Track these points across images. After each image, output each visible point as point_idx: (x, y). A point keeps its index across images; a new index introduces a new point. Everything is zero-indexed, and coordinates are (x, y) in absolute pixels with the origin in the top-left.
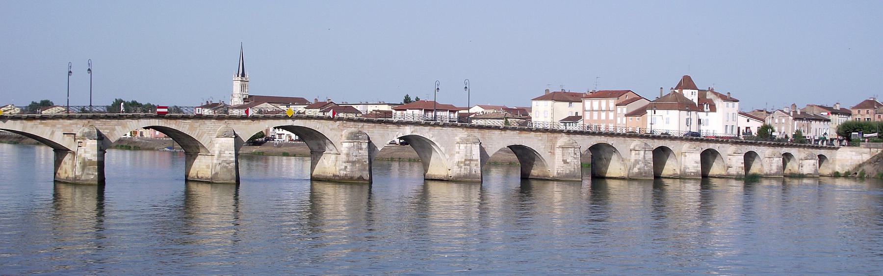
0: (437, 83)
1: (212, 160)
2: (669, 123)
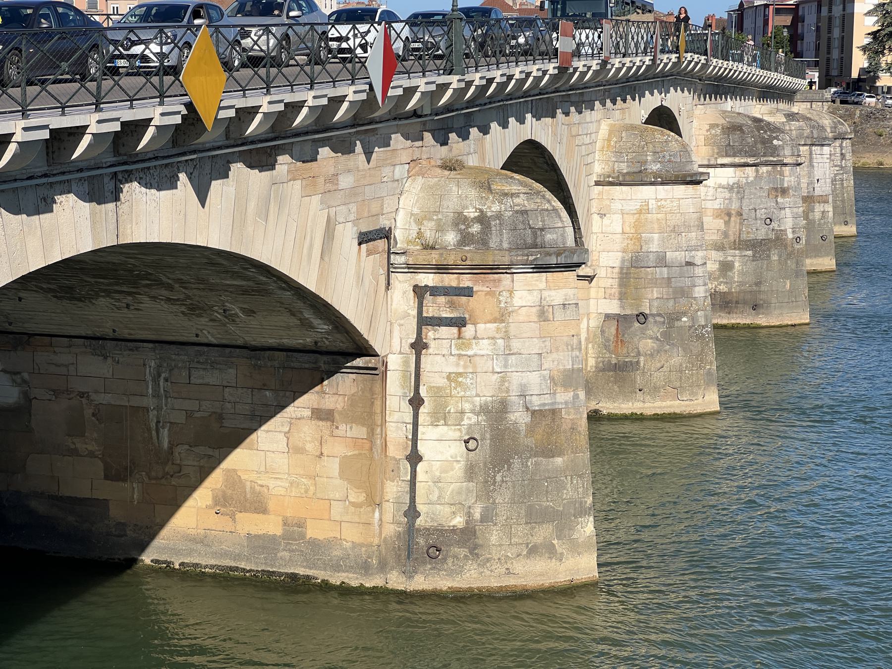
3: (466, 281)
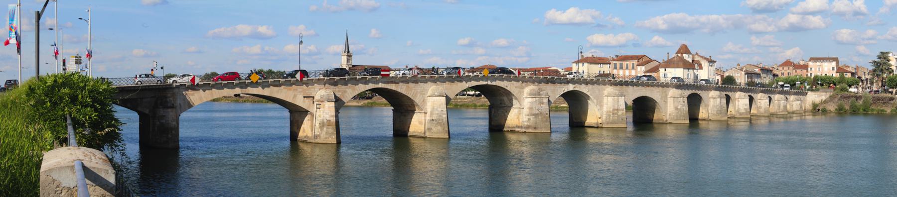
0: (581, 47)
1: (425, 117)
3: (321, 103)
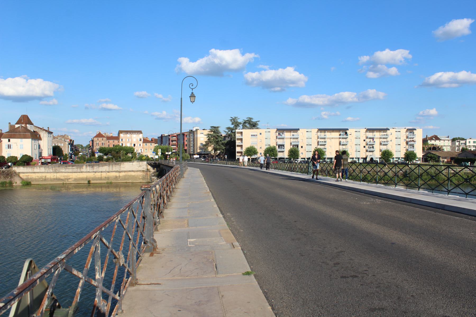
2: (23, 148)
